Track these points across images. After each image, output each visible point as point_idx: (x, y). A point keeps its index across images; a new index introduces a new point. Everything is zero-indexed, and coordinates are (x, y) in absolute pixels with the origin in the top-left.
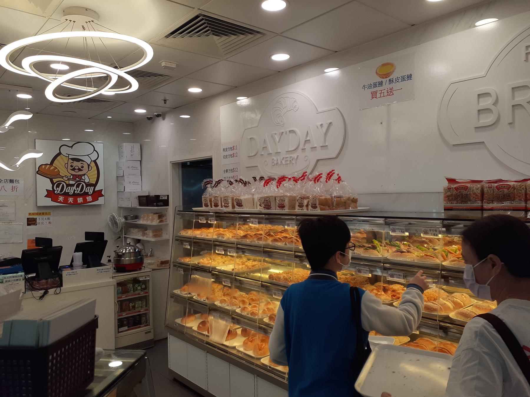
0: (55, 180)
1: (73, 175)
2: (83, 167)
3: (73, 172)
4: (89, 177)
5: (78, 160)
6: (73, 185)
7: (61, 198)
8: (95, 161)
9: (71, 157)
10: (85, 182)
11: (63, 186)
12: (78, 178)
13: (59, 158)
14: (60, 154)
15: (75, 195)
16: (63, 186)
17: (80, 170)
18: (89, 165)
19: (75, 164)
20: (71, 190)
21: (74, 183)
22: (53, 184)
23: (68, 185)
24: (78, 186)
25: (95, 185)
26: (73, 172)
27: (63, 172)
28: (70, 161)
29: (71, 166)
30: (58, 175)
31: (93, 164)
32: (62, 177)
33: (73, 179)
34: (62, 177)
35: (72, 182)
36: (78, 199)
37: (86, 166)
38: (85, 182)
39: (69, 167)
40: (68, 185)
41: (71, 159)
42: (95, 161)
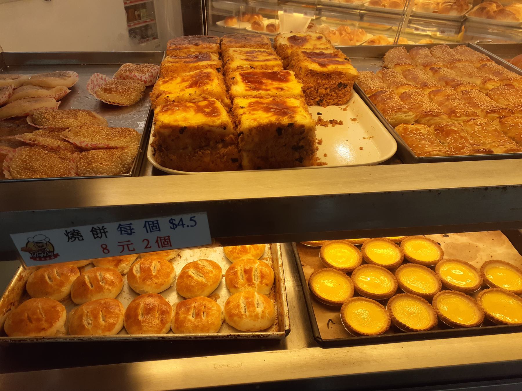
1: (40, 249)
2: (43, 245)
4: (48, 249)
7: (38, 259)
8: (49, 242)
9: (35, 242)
11: (37, 255)
12: (44, 251)
14: (29, 242)
15: (44, 257)
16: (37, 255)
18: (46, 244)
19: (39, 244)
22: (31, 254)
24: (44, 253)
25: (53, 251)
27: (34, 249)
28: (35, 244)
29: (37, 246)
31: (48, 243)
34: (35, 251)
36: (47, 258)
39: (36, 247)
40: (39, 254)
41: (36, 243)
42: (49, 242)
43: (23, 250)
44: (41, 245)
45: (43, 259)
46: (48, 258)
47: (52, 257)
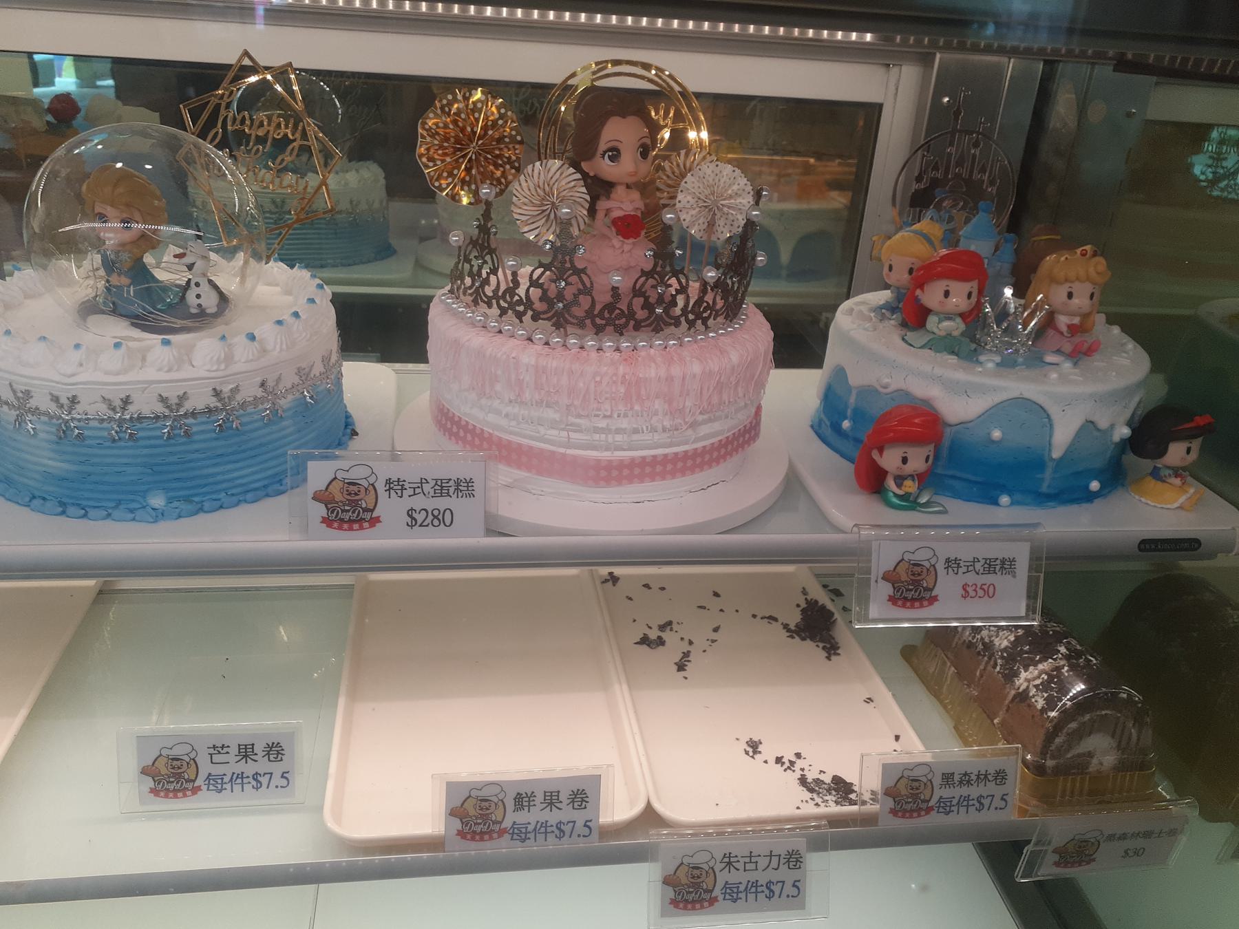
2: (359, 491)
5: (354, 484)
6: (348, 511)
9: (346, 481)
10: (361, 507)
11: (338, 512)
12: (354, 504)
13: (334, 482)
14: (335, 478)
15: (351, 521)
17: (356, 494)
18: (366, 489)
19: (352, 488)
20: (346, 517)
21: (349, 508)
22: (328, 509)
25: (372, 511)
29: (347, 491)
30: (333, 501)
37: (363, 490)
38: (361, 507)
43: (317, 497)
45: (346, 526)
46: (356, 526)
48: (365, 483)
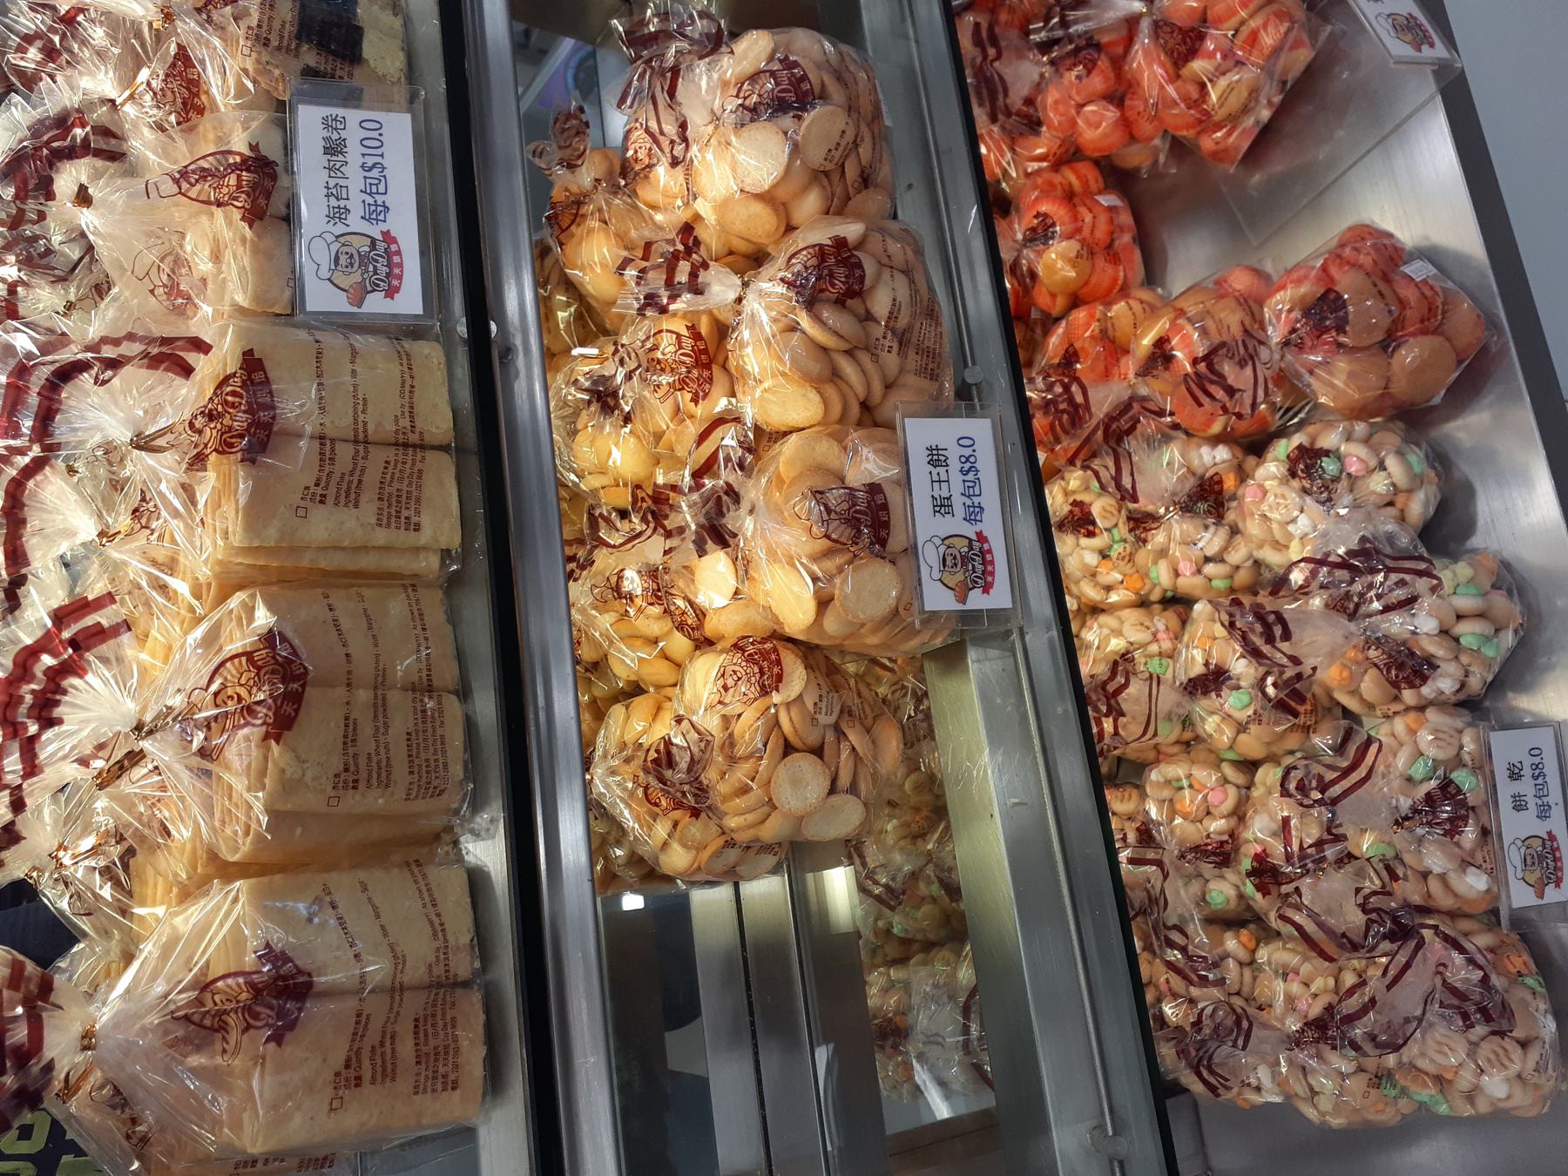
0: (369, 289)
3: (356, 265)
6: (375, 267)
7: (395, 282)
8: (337, 237)
15: (390, 265)
18: (343, 245)
20: (383, 270)
22: (374, 290)
23: (375, 273)
26: (356, 265)
28: (339, 268)
32: (364, 279)
33: (366, 266)
34: (364, 279)
35: (371, 268)
39: (349, 269)
40: (375, 273)
44: (343, 260)
45: (397, 271)
47: (394, 248)
48: (335, 247)
